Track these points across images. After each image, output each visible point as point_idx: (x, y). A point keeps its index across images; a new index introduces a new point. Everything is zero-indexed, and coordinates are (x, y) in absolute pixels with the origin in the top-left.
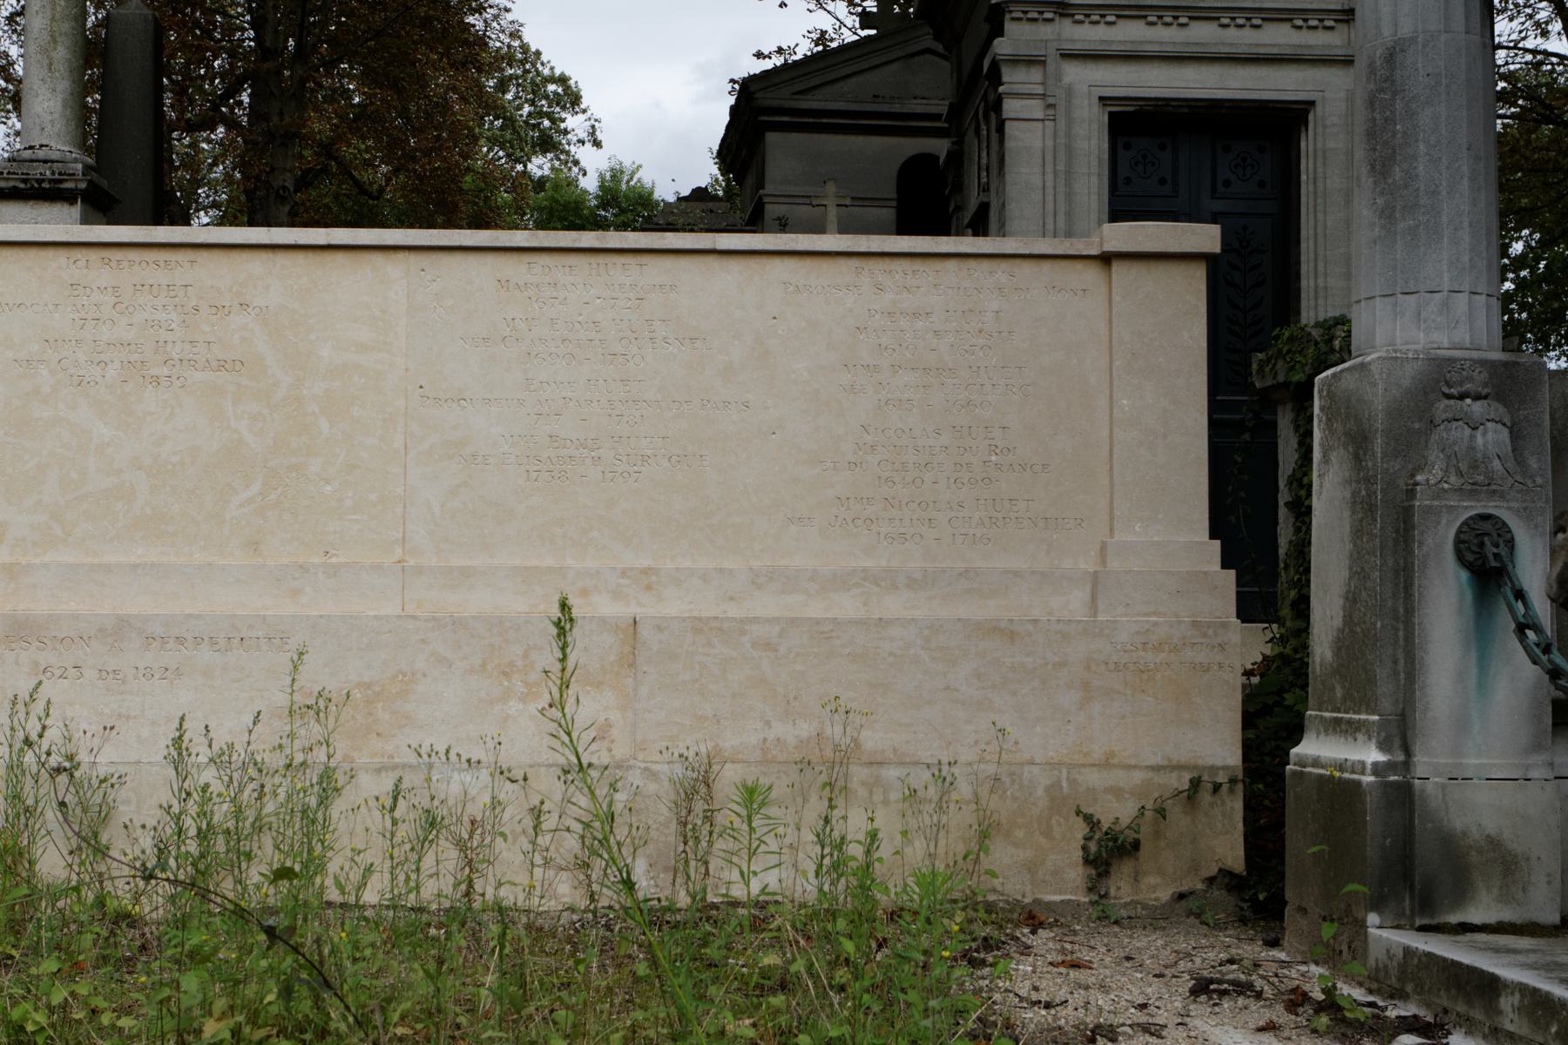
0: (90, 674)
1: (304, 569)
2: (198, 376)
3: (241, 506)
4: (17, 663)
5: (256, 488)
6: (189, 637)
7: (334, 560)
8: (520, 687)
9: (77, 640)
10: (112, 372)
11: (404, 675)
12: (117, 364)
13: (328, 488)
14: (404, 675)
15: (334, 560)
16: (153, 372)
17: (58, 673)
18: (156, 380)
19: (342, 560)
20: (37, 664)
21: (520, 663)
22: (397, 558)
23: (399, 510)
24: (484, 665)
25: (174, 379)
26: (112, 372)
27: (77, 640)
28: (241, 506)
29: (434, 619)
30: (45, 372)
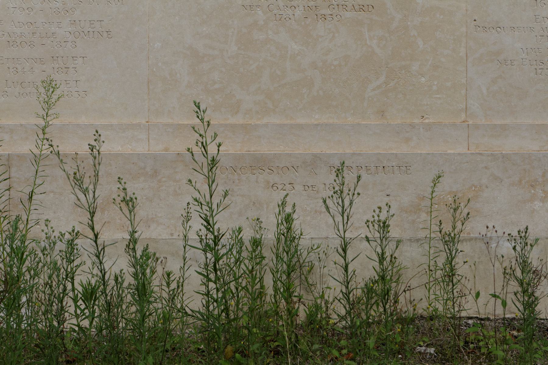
0: (299, 188)
1: (412, 126)
2: (348, 14)
3: (374, 90)
4: (257, 182)
5: (383, 79)
6: (354, 167)
7: (427, 121)
8: (541, 194)
9: (291, 168)
10: (298, 12)
11: (476, 187)
12: (301, 8)
13: (423, 79)
14: (476, 187)
15: (427, 121)
16: (323, 12)
17: (280, 187)
18: (324, 17)
19: (431, 121)
20: (268, 182)
21: (540, 180)
22: (463, 119)
23: (463, 92)
24: (520, 181)
25: (334, 17)
26: (298, 12)
27: (291, 168)
28: (374, 90)
29: (492, 155)
30: (260, 13)
